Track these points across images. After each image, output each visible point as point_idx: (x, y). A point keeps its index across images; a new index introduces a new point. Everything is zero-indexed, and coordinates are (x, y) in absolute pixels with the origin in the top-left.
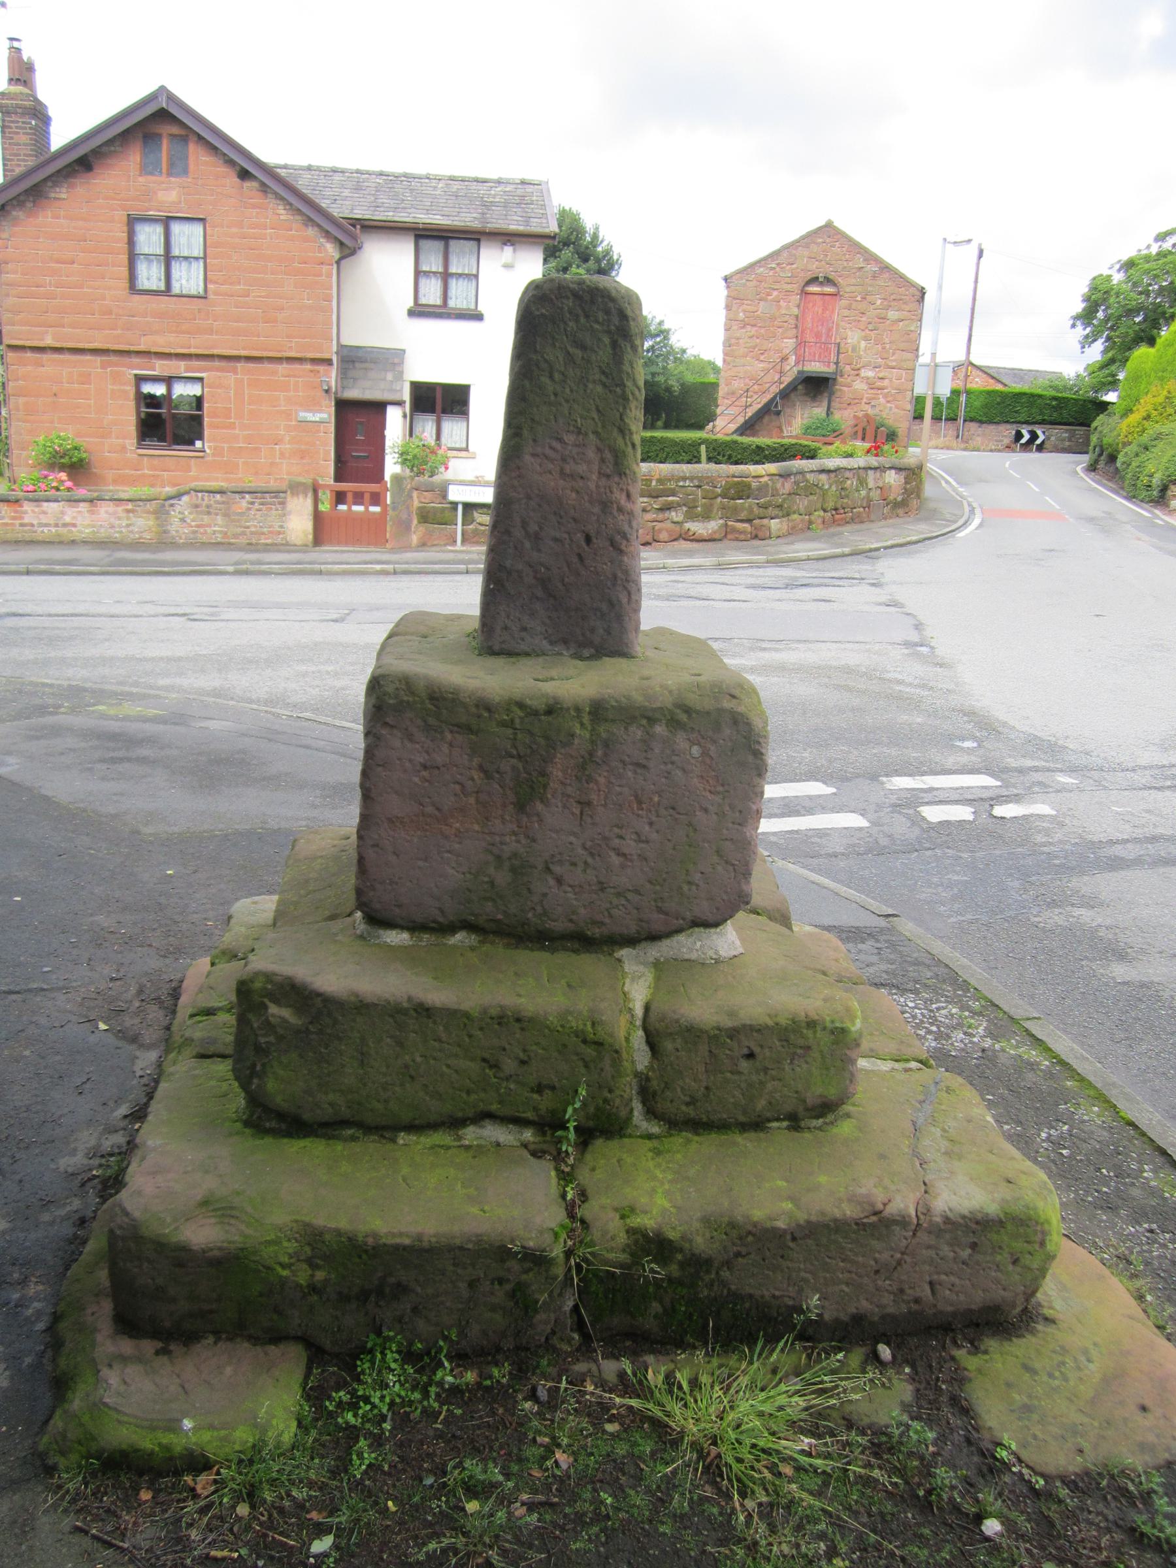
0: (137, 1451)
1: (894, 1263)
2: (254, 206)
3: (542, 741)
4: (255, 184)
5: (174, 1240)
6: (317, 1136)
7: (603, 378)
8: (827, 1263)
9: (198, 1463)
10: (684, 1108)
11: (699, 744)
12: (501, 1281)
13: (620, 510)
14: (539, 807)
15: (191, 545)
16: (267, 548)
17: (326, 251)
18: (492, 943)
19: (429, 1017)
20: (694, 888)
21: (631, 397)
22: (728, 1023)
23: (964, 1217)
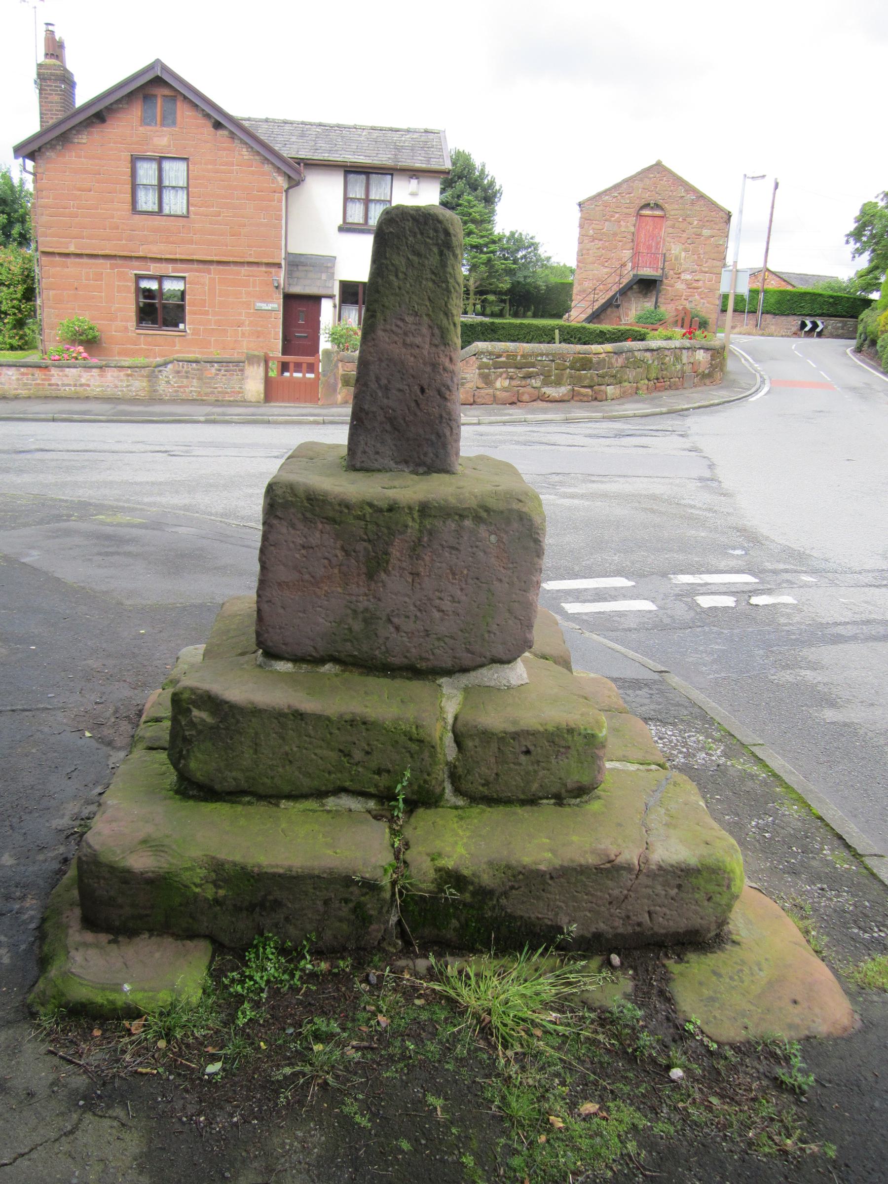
0: (92, 1003)
1: (623, 897)
2: (225, 149)
3: (385, 531)
4: (226, 133)
5: (122, 865)
6: (225, 801)
7: (434, 277)
8: (574, 896)
9: (133, 1013)
10: (481, 788)
11: (495, 534)
12: (346, 901)
13: (445, 369)
14: (383, 576)
15: (174, 401)
16: (231, 404)
17: (278, 182)
18: (351, 672)
19: (302, 720)
20: (492, 635)
21: (453, 290)
22: (512, 729)
23: (672, 866)
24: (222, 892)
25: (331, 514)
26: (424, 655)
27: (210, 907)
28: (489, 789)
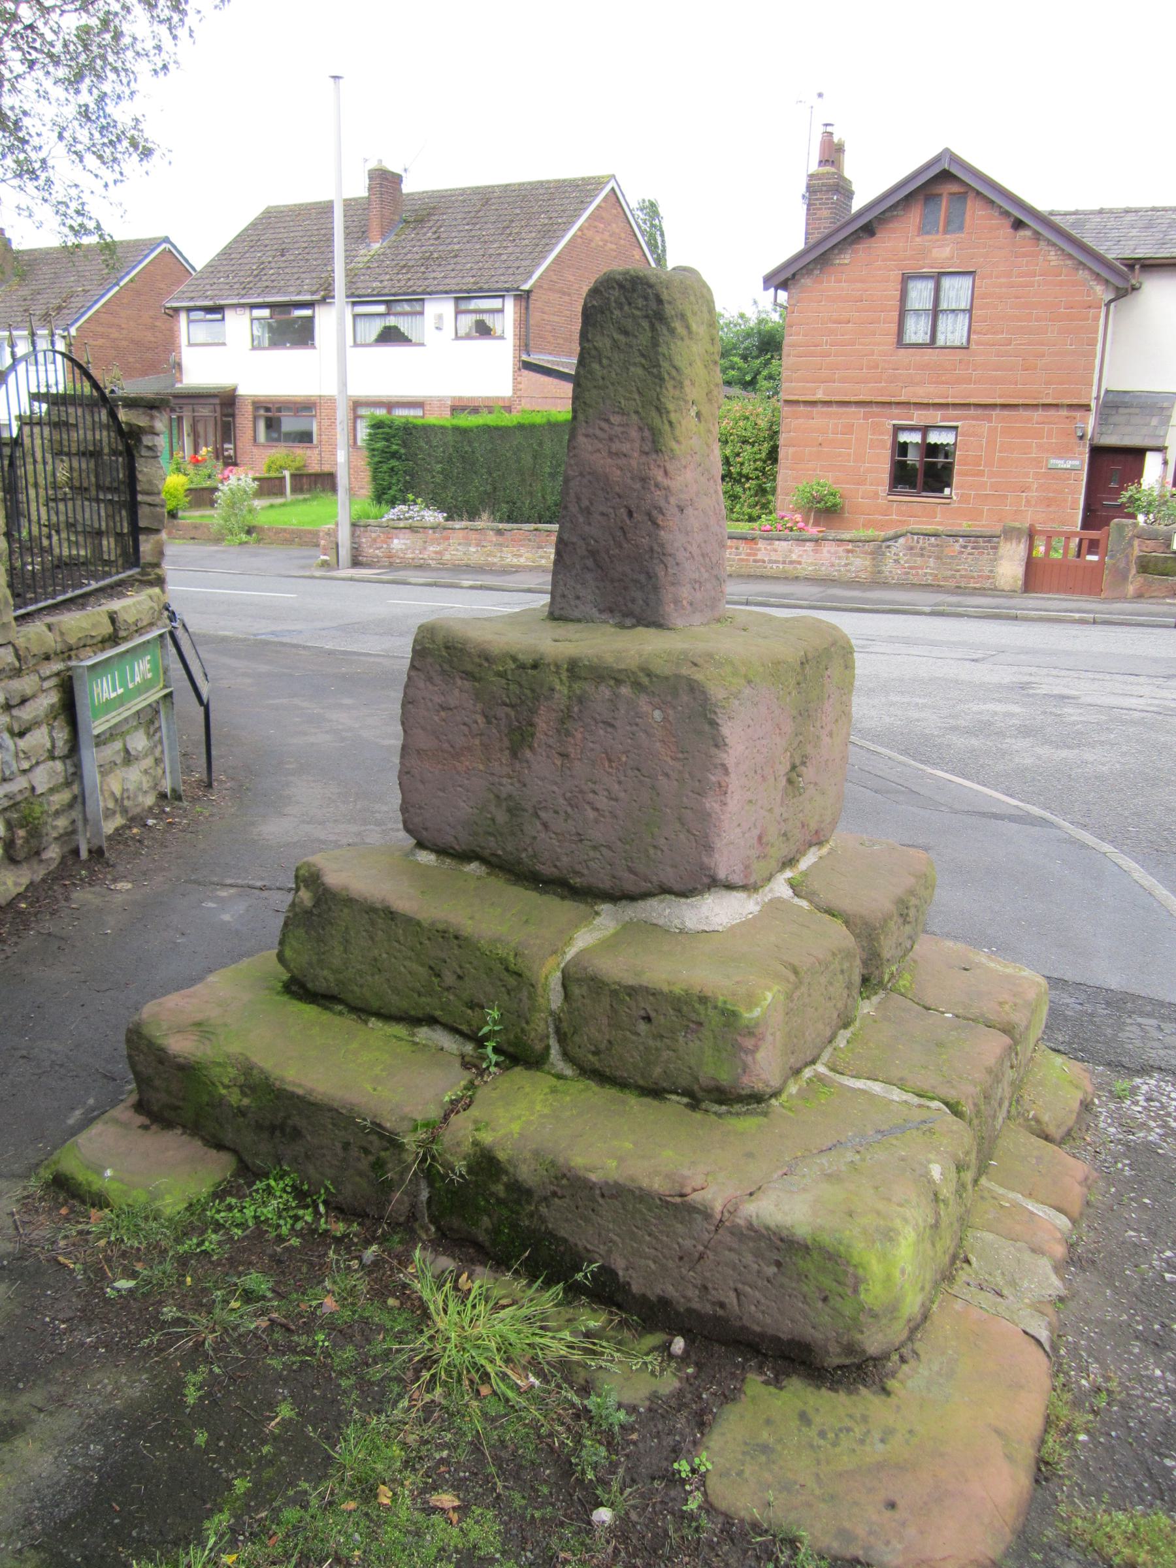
0: (73, 1178)
1: (697, 1255)
2: (1025, 255)
3: (528, 692)
4: (1028, 233)
5: (159, 1042)
6: (318, 1005)
7: (643, 361)
8: (633, 1232)
9: (100, 1201)
10: (590, 1056)
11: (660, 709)
12: (366, 1151)
13: (657, 485)
14: (528, 754)
15: (902, 586)
16: (975, 592)
17: (1095, 293)
18: (497, 876)
19: (392, 919)
20: (659, 853)
21: (666, 377)
22: (631, 981)
23: (768, 1228)
24: (246, 1101)
25: (469, 667)
26: (578, 868)
27: (235, 1116)
28: (600, 1060)
